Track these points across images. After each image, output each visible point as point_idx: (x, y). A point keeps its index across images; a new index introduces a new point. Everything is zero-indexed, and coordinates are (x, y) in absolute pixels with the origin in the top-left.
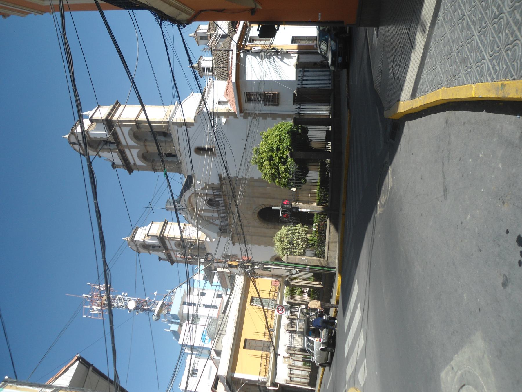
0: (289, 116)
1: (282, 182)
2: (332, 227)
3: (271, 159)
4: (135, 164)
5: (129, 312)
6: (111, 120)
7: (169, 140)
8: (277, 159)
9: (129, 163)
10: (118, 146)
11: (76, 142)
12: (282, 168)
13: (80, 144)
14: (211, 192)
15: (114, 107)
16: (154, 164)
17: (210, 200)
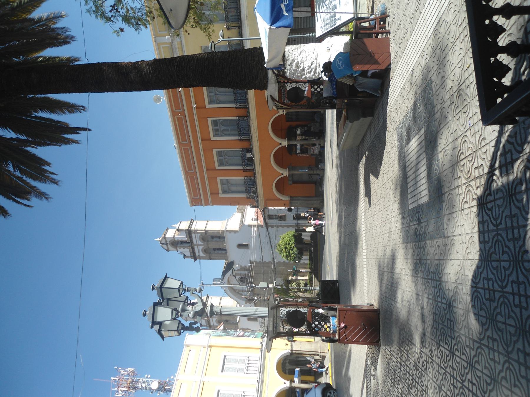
0: (291, 226)
1: (292, 258)
2: (315, 279)
3: (286, 248)
4: (199, 256)
5: (151, 393)
6: (190, 229)
7: (222, 240)
8: (289, 248)
9: (196, 255)
10: (191, 245)
11: (165, 243)
12: (292, 252)
13: (167, 244)
14: (243, 272)
15: (191, 222)
16: (210, 255)
17: (241, 278)
